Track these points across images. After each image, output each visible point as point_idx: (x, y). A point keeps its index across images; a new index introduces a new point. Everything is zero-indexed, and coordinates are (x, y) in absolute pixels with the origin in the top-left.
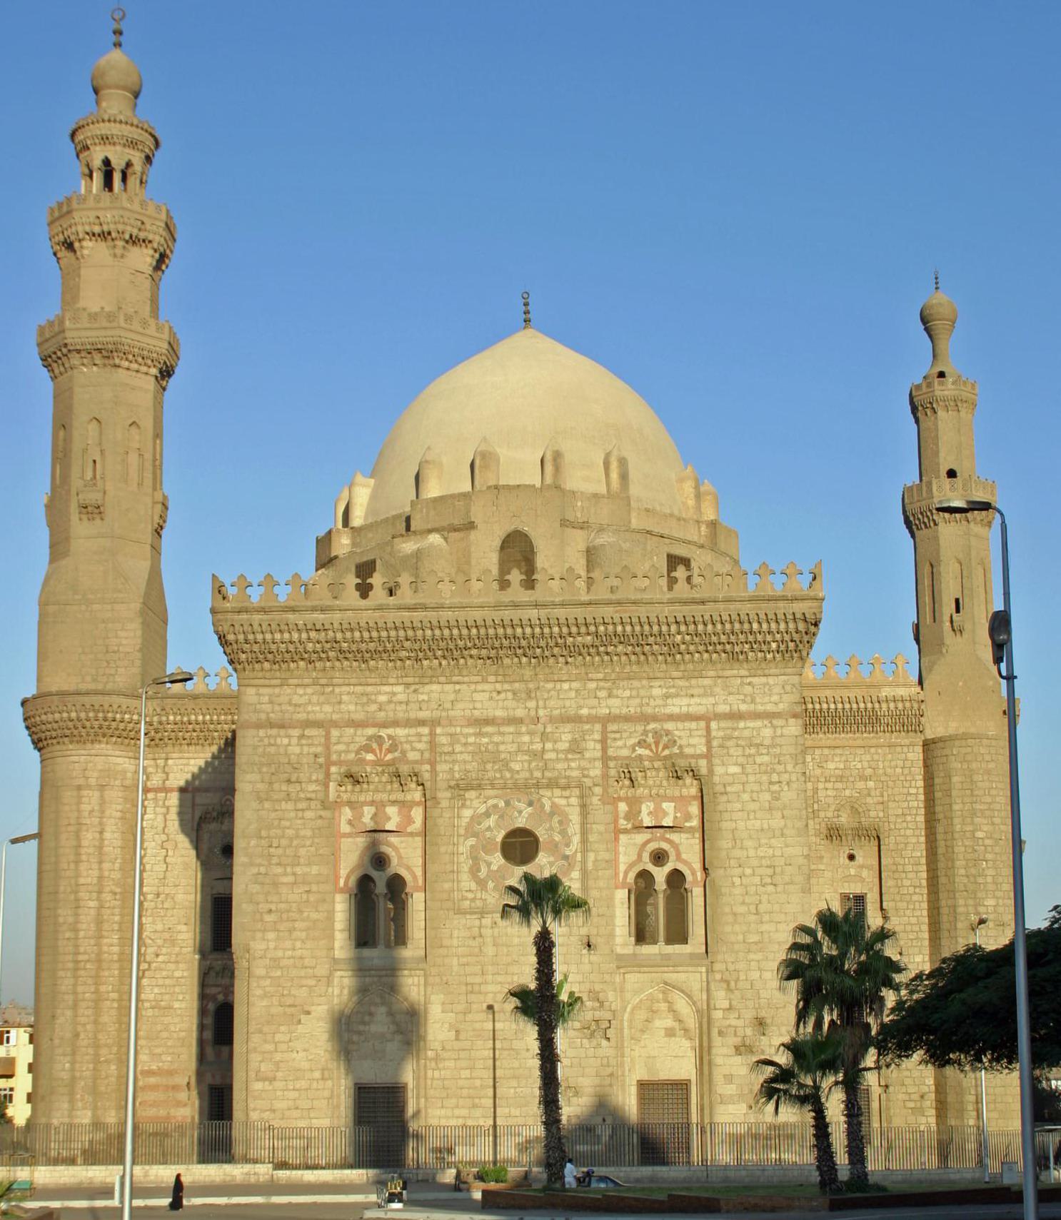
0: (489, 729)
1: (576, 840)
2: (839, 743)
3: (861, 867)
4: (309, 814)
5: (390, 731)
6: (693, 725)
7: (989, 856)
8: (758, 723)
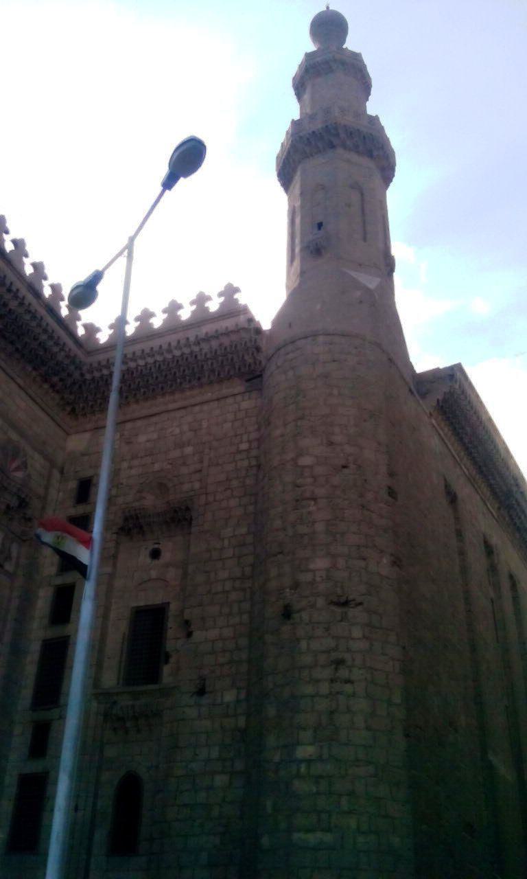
2: (155, 410)
3: (167, 565)
7: (320, 492)
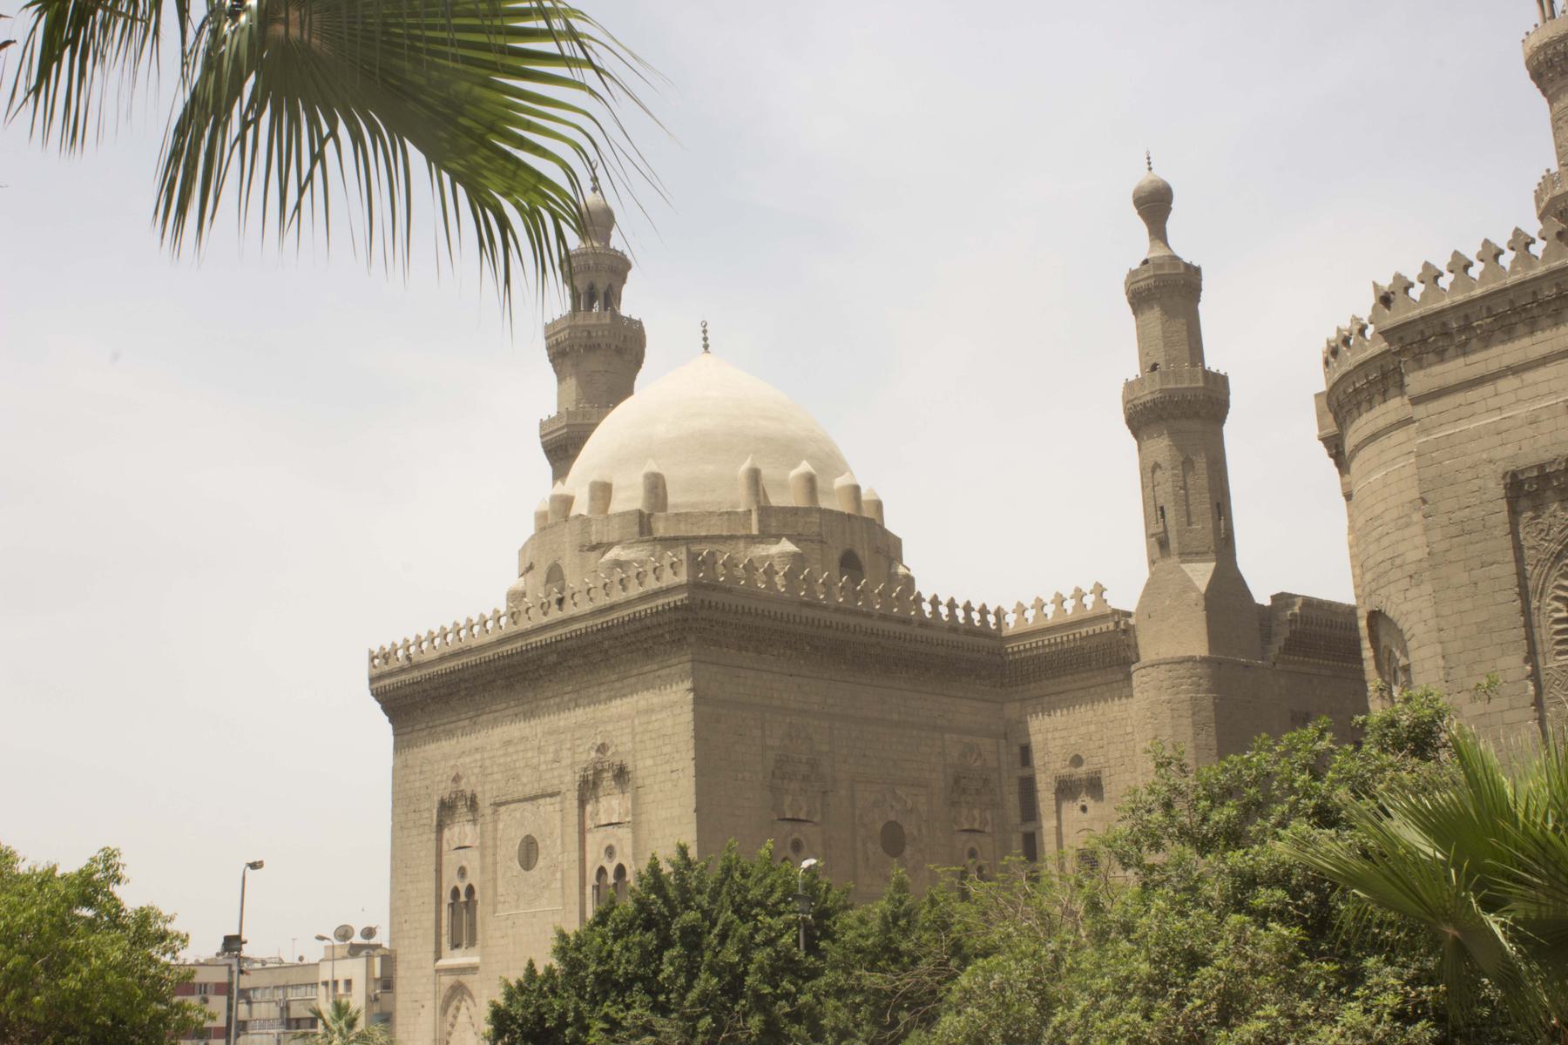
0: (511, 749)
1: (559, 842)
4: (425, 837)
5: (461, 760)
6: (624, 724)
8: (664, 715)
